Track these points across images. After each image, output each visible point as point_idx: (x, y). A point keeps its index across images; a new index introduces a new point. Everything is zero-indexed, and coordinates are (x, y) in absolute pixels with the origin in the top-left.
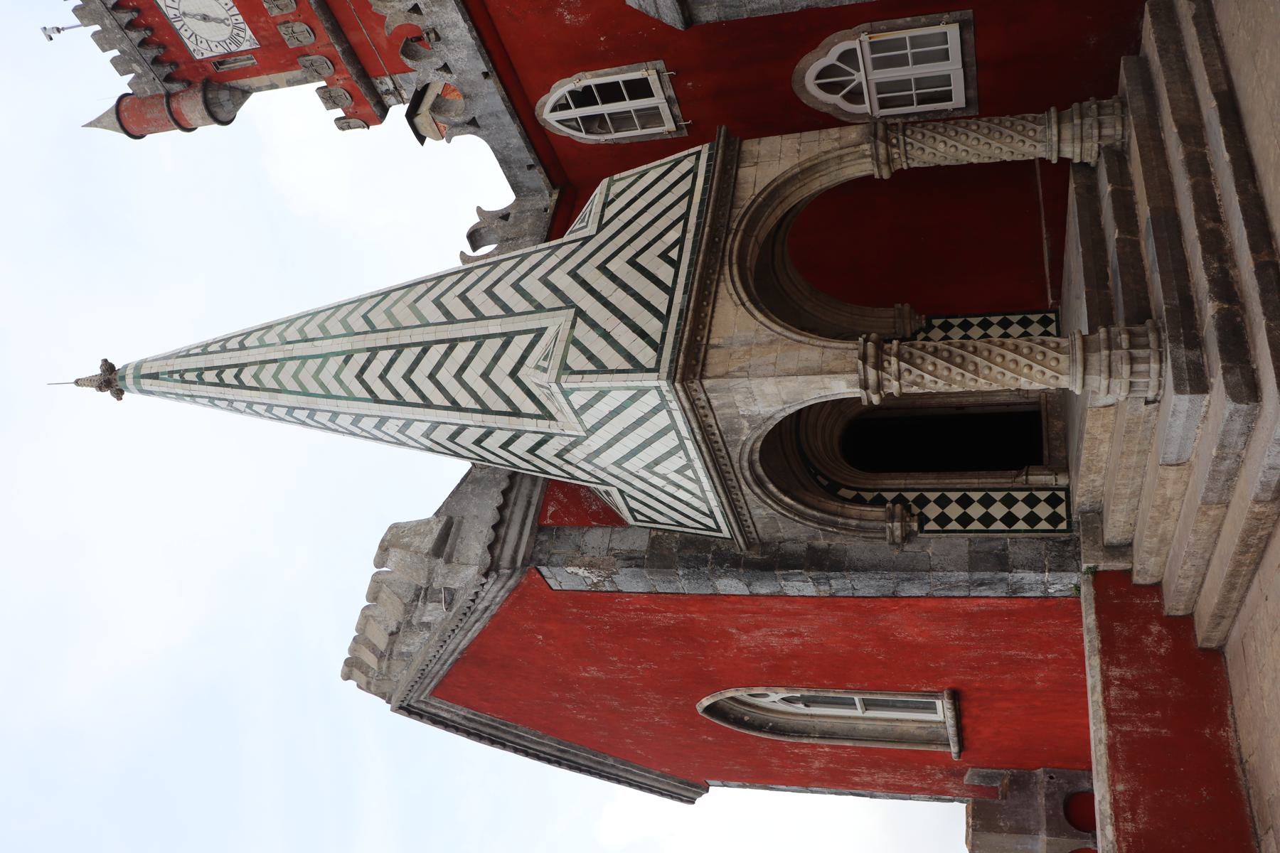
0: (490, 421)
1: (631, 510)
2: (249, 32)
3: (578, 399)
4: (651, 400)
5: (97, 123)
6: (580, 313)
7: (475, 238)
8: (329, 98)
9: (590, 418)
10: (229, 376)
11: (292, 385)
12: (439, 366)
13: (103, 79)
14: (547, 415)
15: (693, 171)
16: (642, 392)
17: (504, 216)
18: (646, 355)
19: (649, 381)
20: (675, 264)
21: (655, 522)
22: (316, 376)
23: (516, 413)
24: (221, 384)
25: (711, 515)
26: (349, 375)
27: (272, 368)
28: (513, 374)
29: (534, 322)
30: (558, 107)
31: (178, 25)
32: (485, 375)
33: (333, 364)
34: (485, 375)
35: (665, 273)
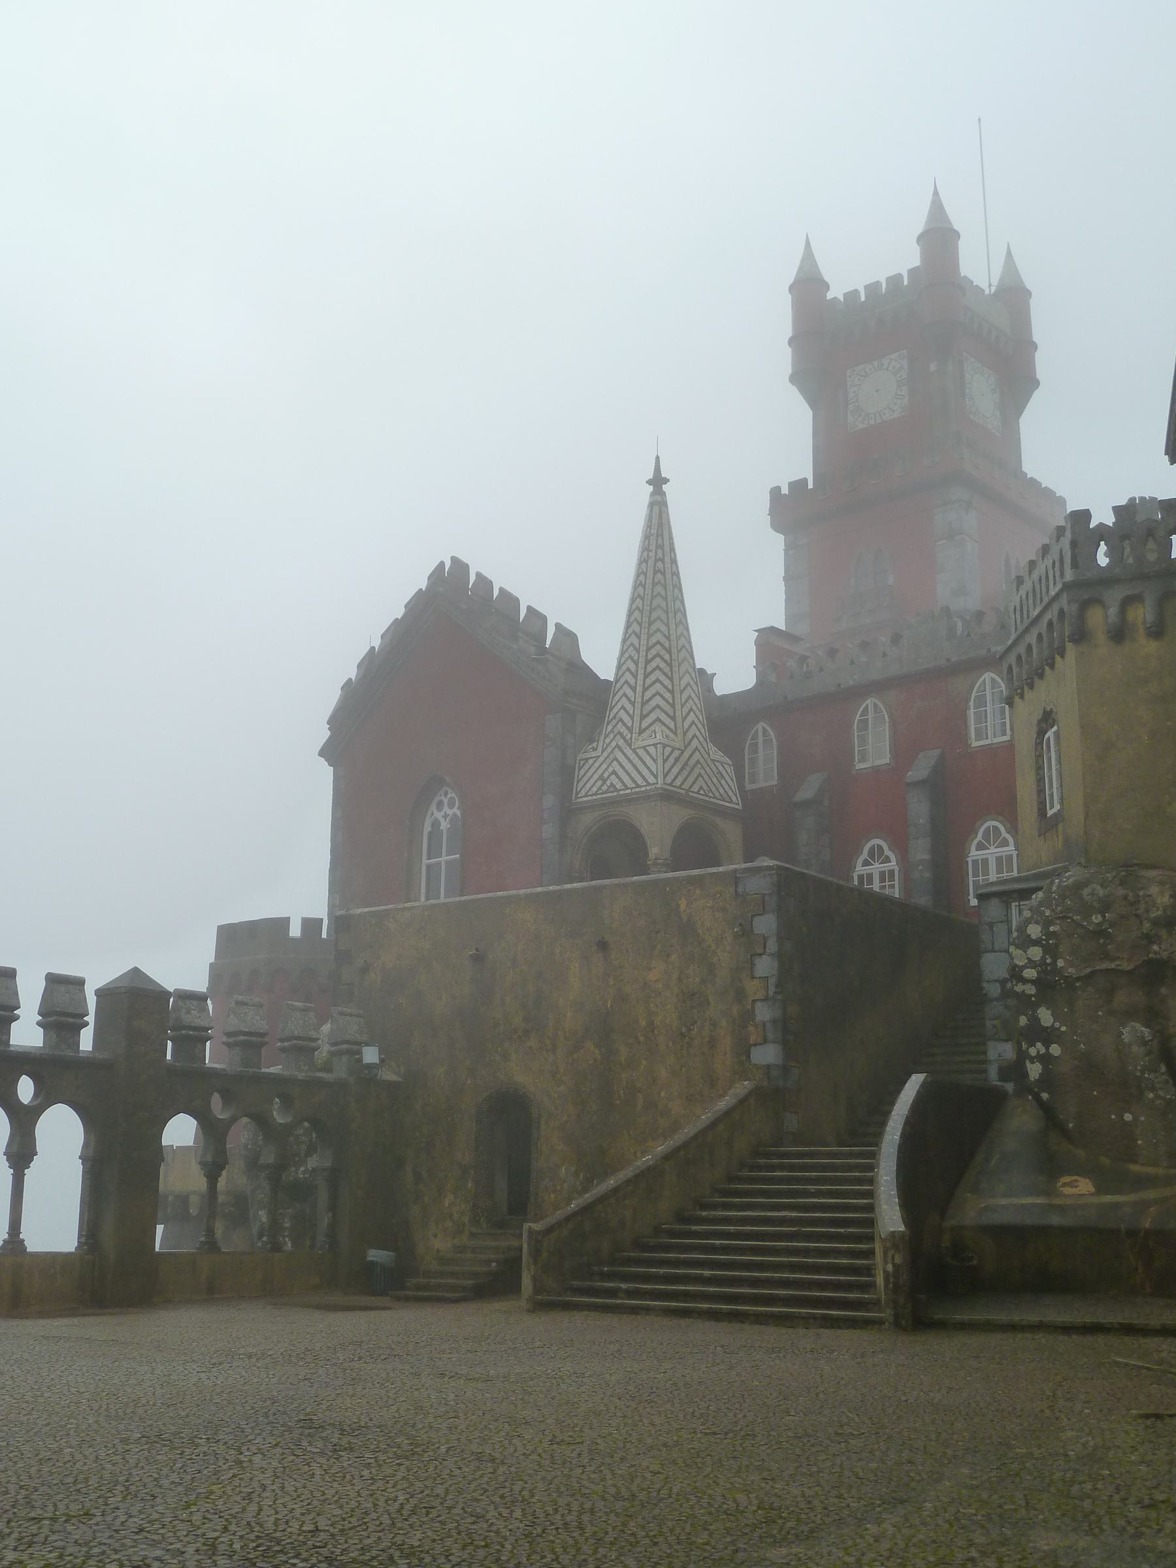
0: (638, 705)
1: (587, 760)
2: (861, 426)
3: (652, 750)
4: (652, 780)
5: (808, 256)
6: (683, 752)
7: (702, 672)
8: (798, 486)
9: (641, 752)
10: (660, 565)
11: (655, 604)
12: (662, 684)
13: (845, 279)
14: (641, 732)
15: (731, 802)
16: (656, 777)
17: (710, 690)
18: (669, 780)
19: (660, 780)
20: (698, 793)
21: (580, 769)
22: (658, 618)
23: (643, 717)
24: (656, 561)
25: (586, 796)
26: (659, 636)
27: (663, 593)
28: (658, 719)
29: (679, 731)
30: (765, 731)
31: (875, 363)
32: (658, 706)
33: (664, 628)
34: (658, 706)
35: (695, 788)
